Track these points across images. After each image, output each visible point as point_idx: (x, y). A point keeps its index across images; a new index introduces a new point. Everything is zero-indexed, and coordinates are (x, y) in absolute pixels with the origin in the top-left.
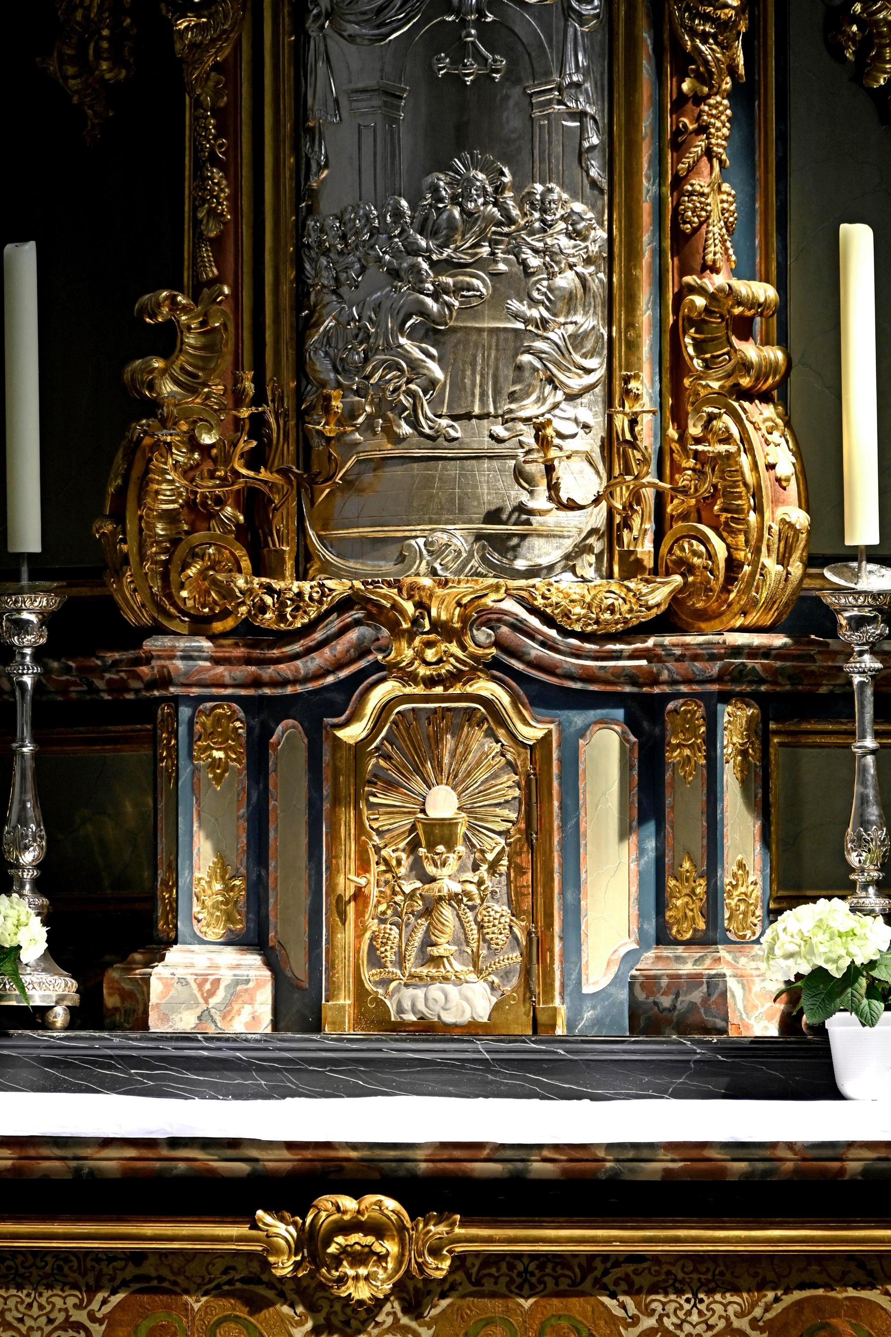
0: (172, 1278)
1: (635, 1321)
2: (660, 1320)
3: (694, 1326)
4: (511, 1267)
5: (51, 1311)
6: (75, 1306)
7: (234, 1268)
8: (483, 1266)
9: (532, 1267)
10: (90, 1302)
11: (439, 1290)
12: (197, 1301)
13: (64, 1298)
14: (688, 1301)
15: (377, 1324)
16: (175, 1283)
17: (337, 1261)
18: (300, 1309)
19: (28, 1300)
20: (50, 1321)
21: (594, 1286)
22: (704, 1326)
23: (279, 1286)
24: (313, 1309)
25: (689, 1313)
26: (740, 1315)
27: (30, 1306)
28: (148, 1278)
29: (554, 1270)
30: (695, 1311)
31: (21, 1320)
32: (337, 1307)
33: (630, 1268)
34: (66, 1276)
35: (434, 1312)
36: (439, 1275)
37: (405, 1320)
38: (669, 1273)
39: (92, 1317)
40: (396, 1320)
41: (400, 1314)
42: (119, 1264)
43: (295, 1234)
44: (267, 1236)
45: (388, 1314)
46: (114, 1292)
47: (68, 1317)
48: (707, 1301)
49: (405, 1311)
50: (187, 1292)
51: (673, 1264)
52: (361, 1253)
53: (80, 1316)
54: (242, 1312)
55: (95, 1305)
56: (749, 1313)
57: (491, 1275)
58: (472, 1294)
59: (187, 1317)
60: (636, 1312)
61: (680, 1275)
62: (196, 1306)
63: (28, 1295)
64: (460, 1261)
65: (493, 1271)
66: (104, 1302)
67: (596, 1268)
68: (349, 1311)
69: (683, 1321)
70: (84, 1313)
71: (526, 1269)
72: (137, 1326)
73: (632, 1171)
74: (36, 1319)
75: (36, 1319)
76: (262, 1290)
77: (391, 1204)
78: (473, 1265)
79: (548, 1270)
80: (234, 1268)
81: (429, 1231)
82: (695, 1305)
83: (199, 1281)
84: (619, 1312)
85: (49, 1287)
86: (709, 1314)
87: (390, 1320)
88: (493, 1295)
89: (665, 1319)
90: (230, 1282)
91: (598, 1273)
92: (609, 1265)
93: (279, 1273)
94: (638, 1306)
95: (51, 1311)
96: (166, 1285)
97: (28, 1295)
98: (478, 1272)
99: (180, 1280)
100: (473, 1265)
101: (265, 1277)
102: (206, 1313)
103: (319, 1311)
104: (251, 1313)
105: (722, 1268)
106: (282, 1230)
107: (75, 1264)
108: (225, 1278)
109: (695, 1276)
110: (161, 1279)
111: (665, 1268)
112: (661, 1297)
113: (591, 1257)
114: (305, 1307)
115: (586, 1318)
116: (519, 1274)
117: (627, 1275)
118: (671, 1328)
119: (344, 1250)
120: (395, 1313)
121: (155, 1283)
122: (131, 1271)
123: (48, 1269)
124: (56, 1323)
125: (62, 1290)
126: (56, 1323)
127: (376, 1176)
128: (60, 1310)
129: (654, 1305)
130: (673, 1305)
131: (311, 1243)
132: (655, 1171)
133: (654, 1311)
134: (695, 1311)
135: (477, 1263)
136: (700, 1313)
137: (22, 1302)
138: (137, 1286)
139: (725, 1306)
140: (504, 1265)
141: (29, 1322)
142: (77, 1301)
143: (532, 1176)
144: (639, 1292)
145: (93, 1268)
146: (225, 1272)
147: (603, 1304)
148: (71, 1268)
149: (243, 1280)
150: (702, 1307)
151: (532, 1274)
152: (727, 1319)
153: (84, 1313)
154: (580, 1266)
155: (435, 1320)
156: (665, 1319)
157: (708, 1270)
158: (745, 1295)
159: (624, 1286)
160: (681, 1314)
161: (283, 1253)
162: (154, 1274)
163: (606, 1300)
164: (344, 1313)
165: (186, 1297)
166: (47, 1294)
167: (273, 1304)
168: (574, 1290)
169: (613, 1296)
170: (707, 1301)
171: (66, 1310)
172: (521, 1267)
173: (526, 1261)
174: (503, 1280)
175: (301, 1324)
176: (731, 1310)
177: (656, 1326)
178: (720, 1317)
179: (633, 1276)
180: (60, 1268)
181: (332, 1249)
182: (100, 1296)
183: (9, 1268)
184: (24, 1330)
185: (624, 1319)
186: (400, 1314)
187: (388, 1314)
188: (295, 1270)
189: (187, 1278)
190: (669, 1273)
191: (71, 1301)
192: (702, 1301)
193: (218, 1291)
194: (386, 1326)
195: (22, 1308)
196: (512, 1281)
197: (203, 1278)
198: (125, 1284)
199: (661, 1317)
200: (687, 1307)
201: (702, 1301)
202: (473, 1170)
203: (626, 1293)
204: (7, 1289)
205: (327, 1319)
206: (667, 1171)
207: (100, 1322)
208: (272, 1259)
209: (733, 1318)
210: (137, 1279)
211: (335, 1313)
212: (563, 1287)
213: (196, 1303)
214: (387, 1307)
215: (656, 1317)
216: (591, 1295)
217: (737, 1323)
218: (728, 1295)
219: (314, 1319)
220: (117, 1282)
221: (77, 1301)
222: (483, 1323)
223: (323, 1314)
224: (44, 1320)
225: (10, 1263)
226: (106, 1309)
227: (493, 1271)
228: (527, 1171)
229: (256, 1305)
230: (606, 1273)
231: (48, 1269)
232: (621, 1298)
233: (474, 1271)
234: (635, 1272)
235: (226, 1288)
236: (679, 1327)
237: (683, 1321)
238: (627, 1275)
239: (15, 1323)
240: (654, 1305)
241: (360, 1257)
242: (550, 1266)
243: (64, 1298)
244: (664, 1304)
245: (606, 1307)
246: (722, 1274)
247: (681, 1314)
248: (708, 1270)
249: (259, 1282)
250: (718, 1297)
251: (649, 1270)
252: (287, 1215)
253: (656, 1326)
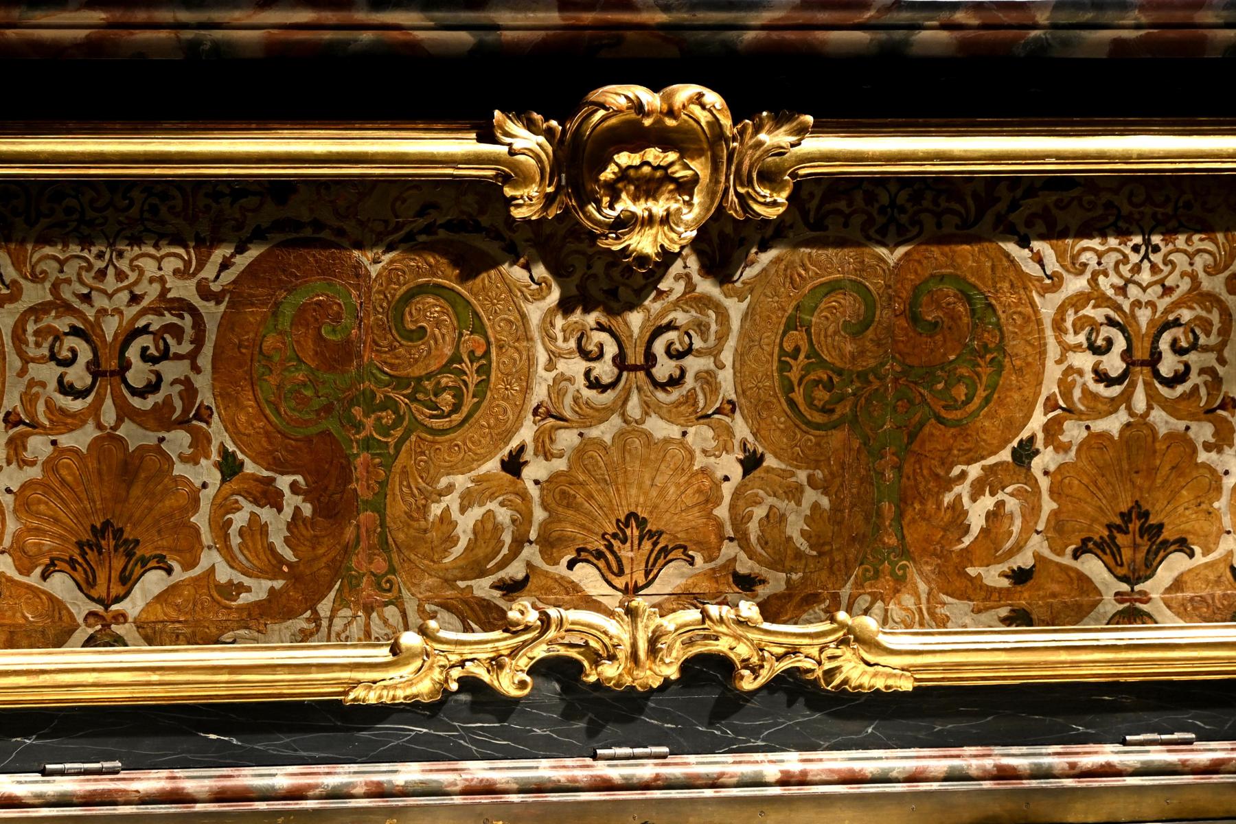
0: (336, 223)
1: (1056, 282)
2: (1093, 280)
3: (1144, 290)
4: (870, 198)
5: (136, 283)
6: (176, 272)
7: (435, 206)
8: (825, 199)
9: (902, 198)
10: (201, 265)
11: (758, 237)
12: (376, 261)
13: (159, 260)
14: (1136, 249)
15: (661, 293)
16: (341, 232)
17: (614, 192)
18: (540, 271)
19: (100, 264)
20: (135, 299)
21: (995, 228)
22: (1158, 289)
23: (507, 234)
24: (559, 271)
25: (1137, 269)
26: (1211, 271)
27: (102, 274)
28: (297, 225)
29: (935, 202)
30: (1146, 265)
31: (86, 298)
32: (599, 267)
33: (1051, 198)
34: (163, 223)
35: (750, 273)
36: (772, 213)
37: (706, 287)
38: (1109, 205)
39: (204, 292)
40: (690, 286)
41: (696, 278)
42: (253, 201)
43: (550, 149)
44: (512, 153)
45: (677, 278)
46: (240, 250)
47: (164, 291)
48: (1164, 250)
49: (707, 270)
50: (360, 246)
51: (1116, 192)
52: (649, 180)
53: (184, 290)
54: (447, 277)
55: (209, 272)
56: (1226, 267)
57: (838, 212)
58: (808, 243)
59: (357, 287)
60: (1058, 268)
61: (1126, 209)
62: (374, 270)
63: (100, 256)
64: (803, 191)
65: (842, 205)
66: (225, 265)
67: (998, 199)
68: (616, 273)
69: (1128, 281)
70: (192, 284)
71: (893, 203)
72: (277, 305)
73: (1065, 43)
74: (110, 296)
75: (110, 296)
76: (481, 243)
77: (713, 98)
78: (812, 195)
79: (926, 203)
80: (435, 206)
81: (760, 144)
82: (1146, 256)
83: (379, 227)
84: (1032, 269)
85: (136, 241)
86: (1166, 269)
87: (680, 288)
88: (841, 243)
89: (1101, 279)
90: (429, 229)
91: (1001, 207)
92: (1019, 193)
93: (518, 214)
94: (1060, 256)
95: (136, 283)
96: (325, 234)
97: (100, 256)
98: (819, 208)
99: (349, 226)
100: (812, 195)
101: (485, 221)
102: (390, 281)
103: (569, 275)
104: (464, 278)
105: (1188, 196)
106: (524, 140)
107: (179, 202)
108: (422, 222)
109: (1148, 210)
110: (318, 225)
111: (1105, 197)
112: (1095, 243)
113: (993, 182)
114: (548, 267)
115: (981, 278)
116: (882, 210)
117: (1046, 208)
118: (1110, 292)
119: (624, 174)
120: (688, 277)
121: (308, 232)
122: (271, 212)
123: (134, 212)
124: (145, 303)
125: (156, 246)
126: (145, 303)
127: (673, 52)
128: (151, 281)
129: (1084, 258)
130: (1115, 256)
131: (577, 165)
132: (1099, 44)
133: (1085, 265)
134: (1146, 265)
135: (818, 193)
136: (1154, 268)
137: (90, 267)
138: (280, 237)
139: (1191, 256)
140: (859, 197)
141: (100, 301)
142: (180, 265)
143: (915, 51)
144: (1063, 235)
145: (208, 208)
146: (421, 213)
147: (1007, 255)
148: (171, 209)
149: (448, 226)
150: (1157, 258)
151: (902, 210)
152: (1194, 277)
153: (192, 284)
154: (975, 196)
155: (751, 287)
156: (1101, 279)
157: (1168, 199)
158: (1220, 237)
159: (1041, 227)
160: (1125, 270)
161: (532, 181)
162: (306, 217)
163: (1011, 248)
164: (608, 276)
165: (356, 253)
166: (131, 252)
167: (495, 264)
168: (967, 233)
169: (1024, 243)
170: (1164, 250)
171: (162, 280)
172: (884, 199)
173: (893, 188)
174: (857, 220)
175: (540, 296)
176: (1199, 262)
177: (1088, 289)
178: (1183, 275)
179: (1055, 211)
180: (154, 210)
181: (609, 174)
182: (219, 254)
183: (69, 211)
184: (91, 314)
185: (1040, 280)
186: (696, 278)
187: (677, 278)
188: (546, 207)
189: (361, 223)
190: (1109, 205)
191: (171, 264)
192: (1156, 249)
193: (409, 243)
194: (673, 297)
195: (88, 278)
196: (871, 220)
197: (386, 222)
198: (258, 236)
199: (1095, 276)
200: (1135, 258)
201: (1156, 249)
202: (824, 43)
203: (1042, 237)
204: (66, 245)
205: (581, 287)
206: (1117, 42)
207: (217, 298)
208: (508, 192)
209: (1202, 275)
210: (279, 225)
211: (595, 276)
212: (947, 230)
213: (375, 263)
214: (677, 268)
215: (1088, 275)
216: (990, 241)
217: (1207, 284)
218: (1196, 237)
219: (562, 286)
220: (246, 233)
221: (180, 265)
222: (825, 290)
223: (576, 279)
224: (124, 296)
225: (72, 202)
226: (228, 276)
227: (842, 205)
228: (906, 43)
229: (471, 265)
230: (1014, 206)
231: (134, 212)
232: (1037, 245)
233: (814, 203)
234: (1058, 204)
235: (422, 238)
236: (1122, 290)
237: (1128, 281)
238: (1046, 208)
239: (77, 304)
240: (1084, 258)
241: (648, 186)
242: (929, 195)
243: (159, 260)
244: (1100, 255)
245: (1012, 261)
246: (1188, 206)
247: (1125, 270)
248: (1168, 199)
249: (477, 228)
250: (1181, 240)
251: (1080, 199)
252: (537, 117)
253: (1088, 289)
